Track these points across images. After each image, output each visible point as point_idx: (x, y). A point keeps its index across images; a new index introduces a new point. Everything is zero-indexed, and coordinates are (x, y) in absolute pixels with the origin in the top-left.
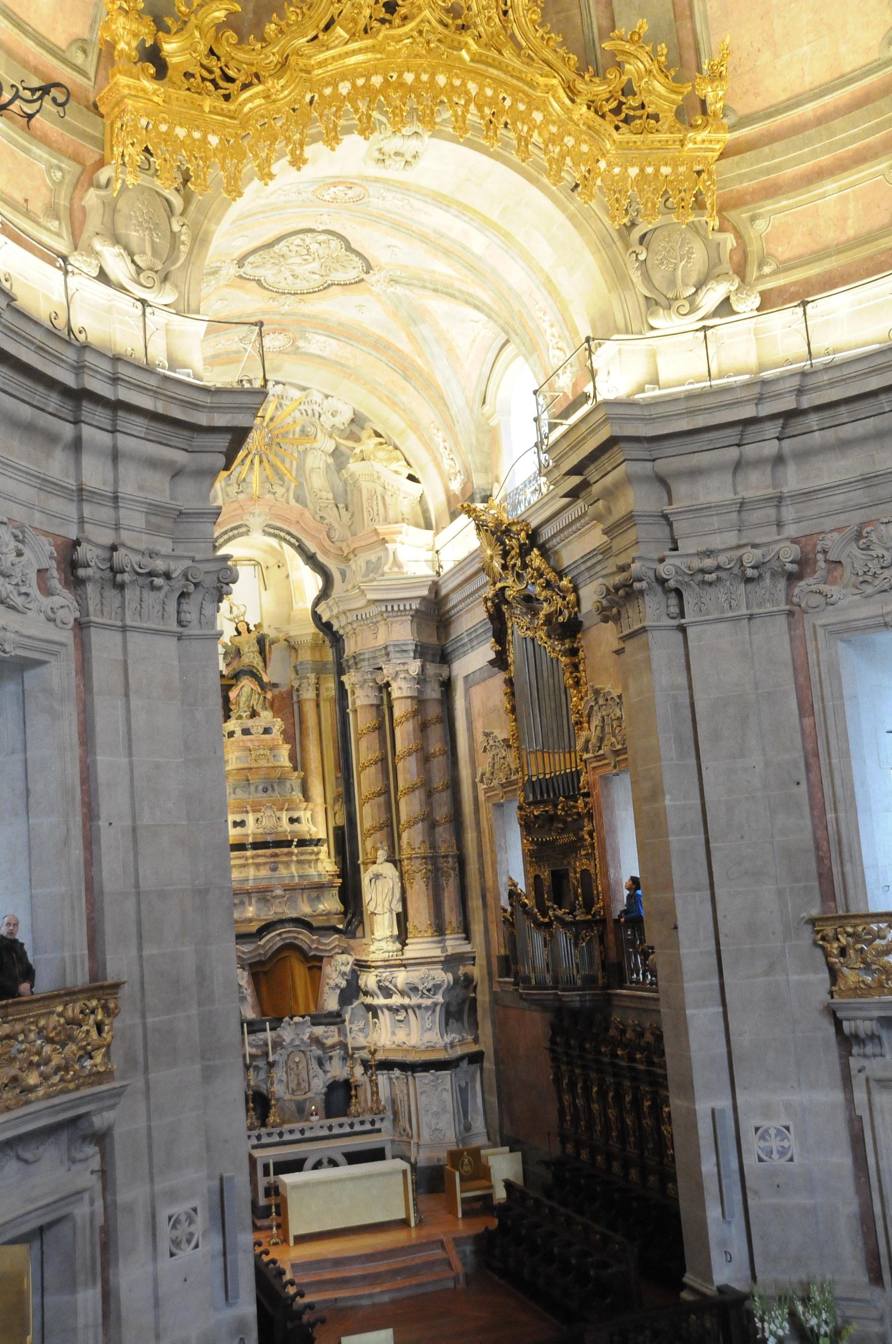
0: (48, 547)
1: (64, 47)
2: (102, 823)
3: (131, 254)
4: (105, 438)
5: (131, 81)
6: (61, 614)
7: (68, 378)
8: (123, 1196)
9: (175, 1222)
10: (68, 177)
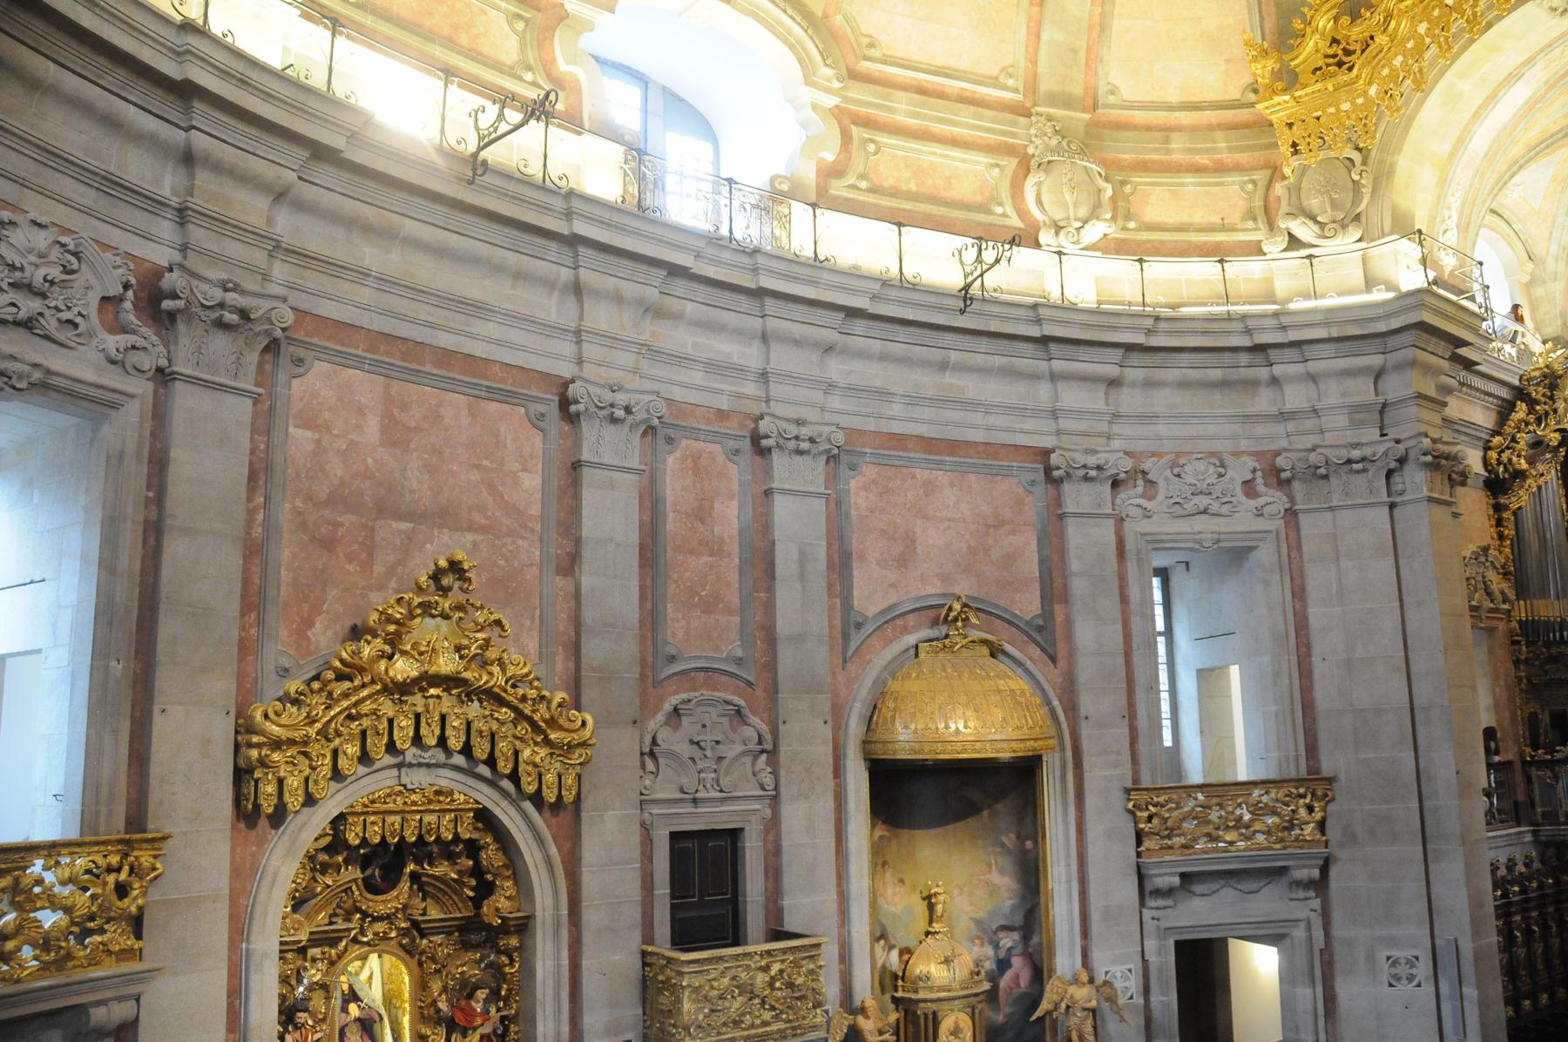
0: (1251, 463)
1: (1237, 96)
2: (1316, 659)
3: (1313, 219)
4: (1298, 369)
5: (1266, 104)
6: (1267, 510)
7: (1244, 341)
8: (1338, 931)
9: (1395, 963)
10: (1262, 184)
